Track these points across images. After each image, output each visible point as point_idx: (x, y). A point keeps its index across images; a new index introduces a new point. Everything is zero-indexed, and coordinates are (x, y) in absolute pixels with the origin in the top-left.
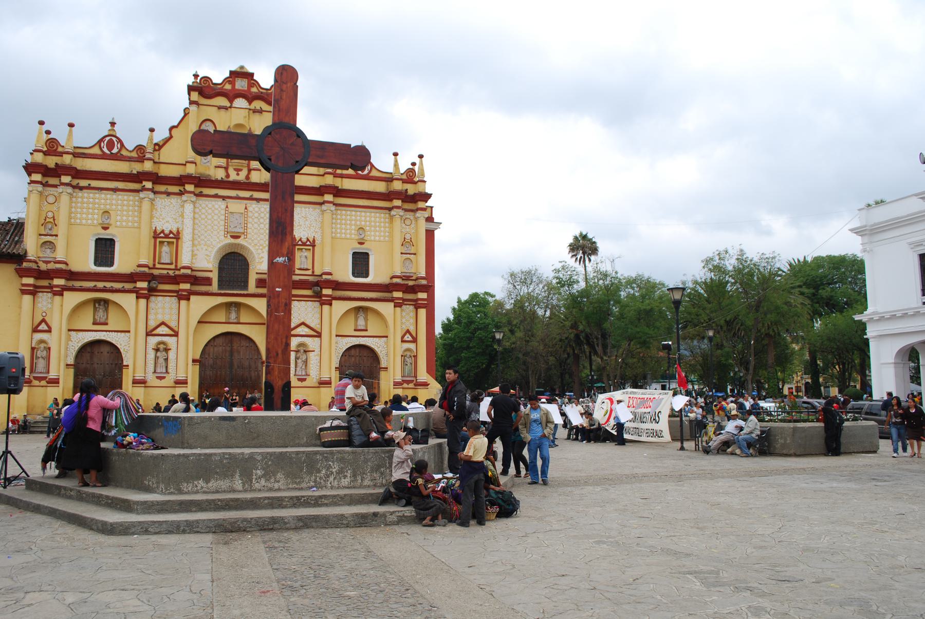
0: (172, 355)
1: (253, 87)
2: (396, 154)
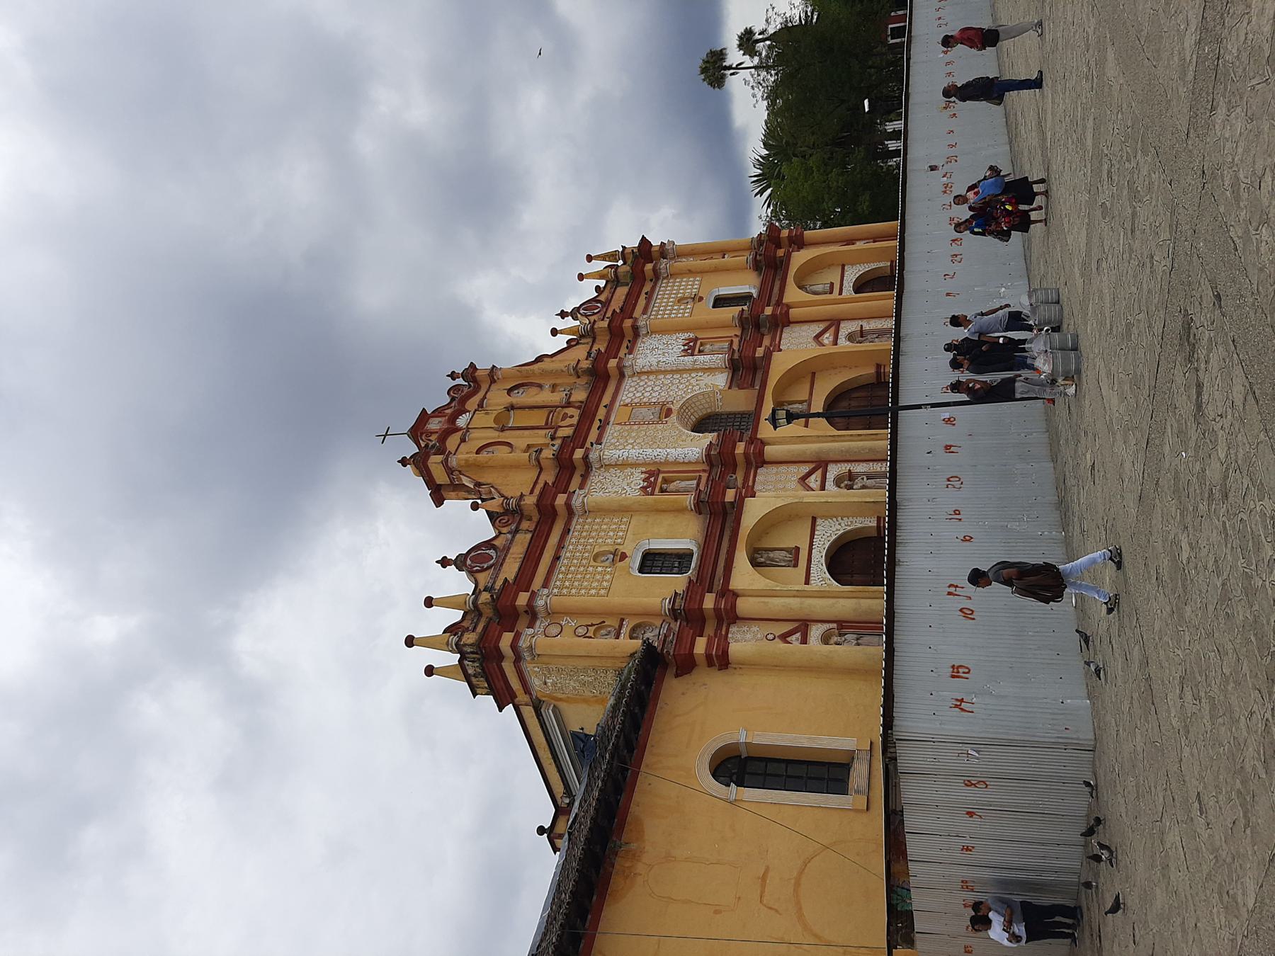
0: (859, 468)
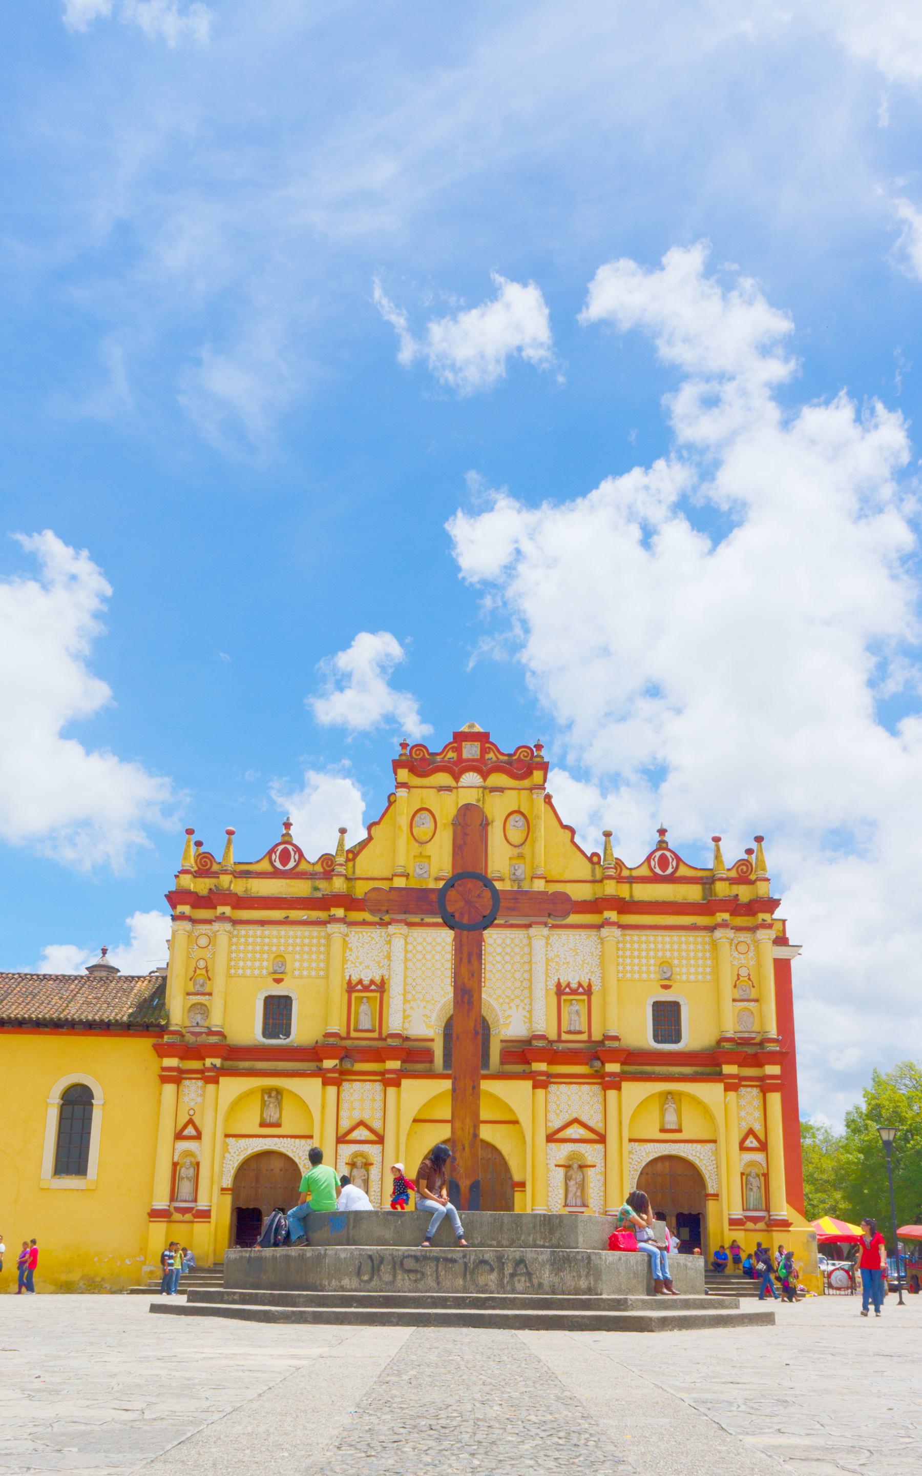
1: (489, 753)
2: (717, 840)
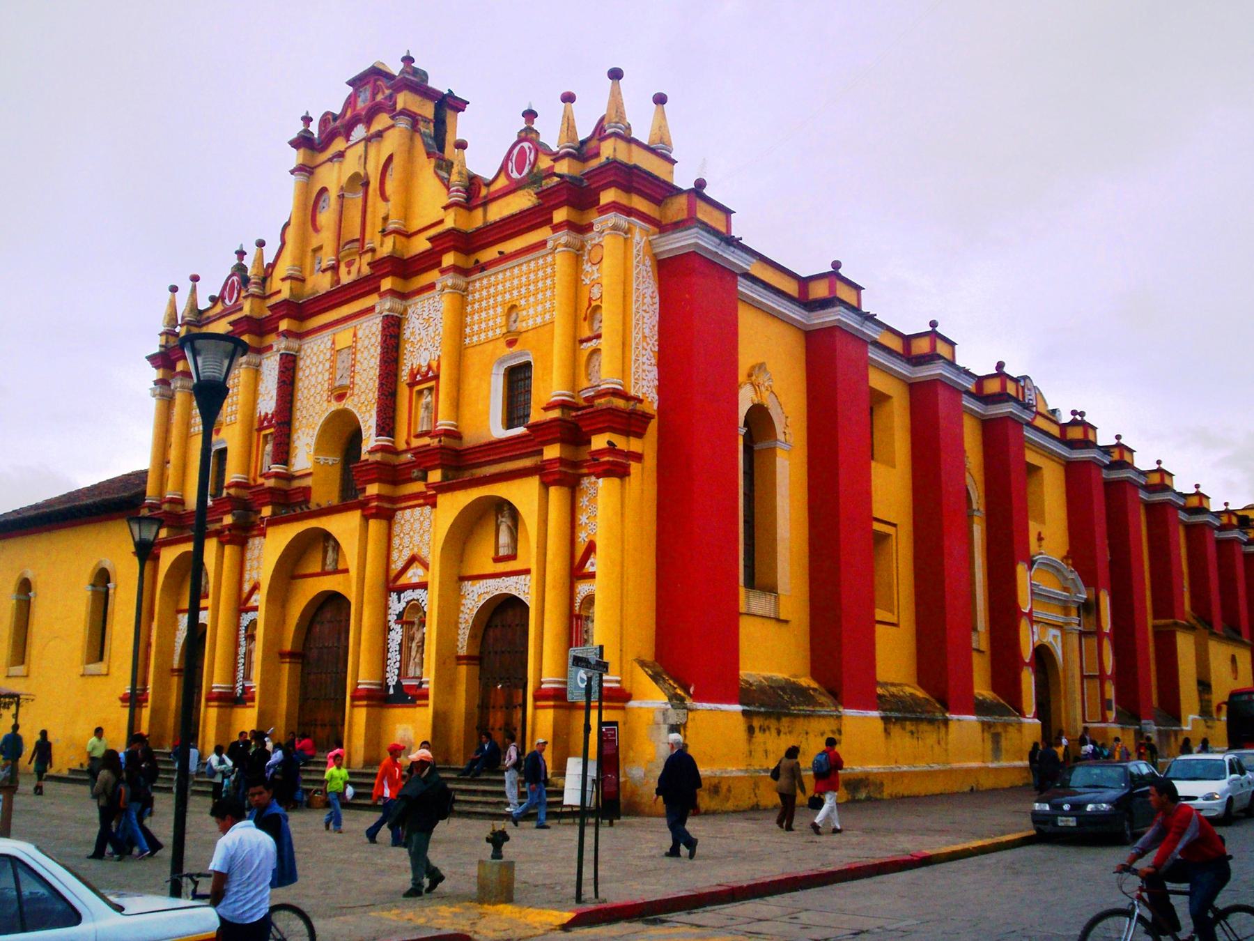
1: (377, 93)
